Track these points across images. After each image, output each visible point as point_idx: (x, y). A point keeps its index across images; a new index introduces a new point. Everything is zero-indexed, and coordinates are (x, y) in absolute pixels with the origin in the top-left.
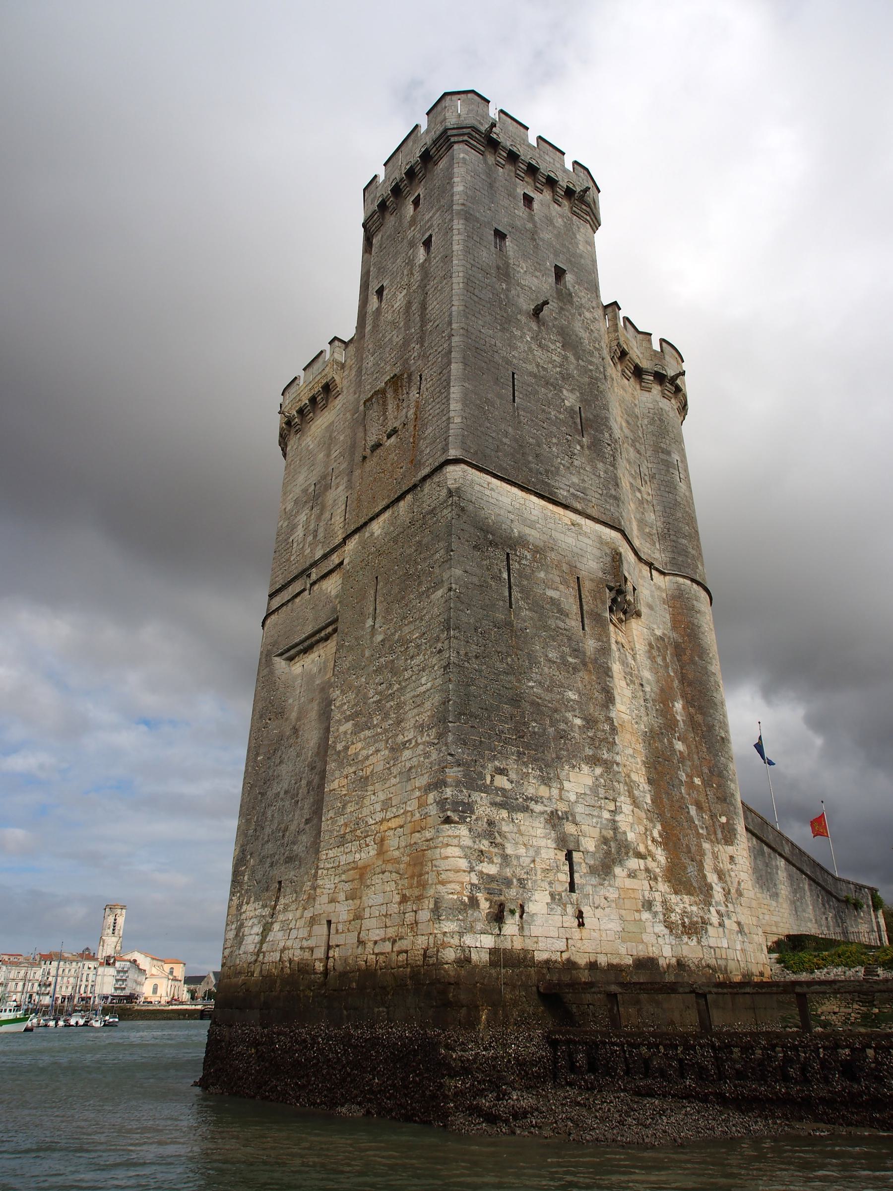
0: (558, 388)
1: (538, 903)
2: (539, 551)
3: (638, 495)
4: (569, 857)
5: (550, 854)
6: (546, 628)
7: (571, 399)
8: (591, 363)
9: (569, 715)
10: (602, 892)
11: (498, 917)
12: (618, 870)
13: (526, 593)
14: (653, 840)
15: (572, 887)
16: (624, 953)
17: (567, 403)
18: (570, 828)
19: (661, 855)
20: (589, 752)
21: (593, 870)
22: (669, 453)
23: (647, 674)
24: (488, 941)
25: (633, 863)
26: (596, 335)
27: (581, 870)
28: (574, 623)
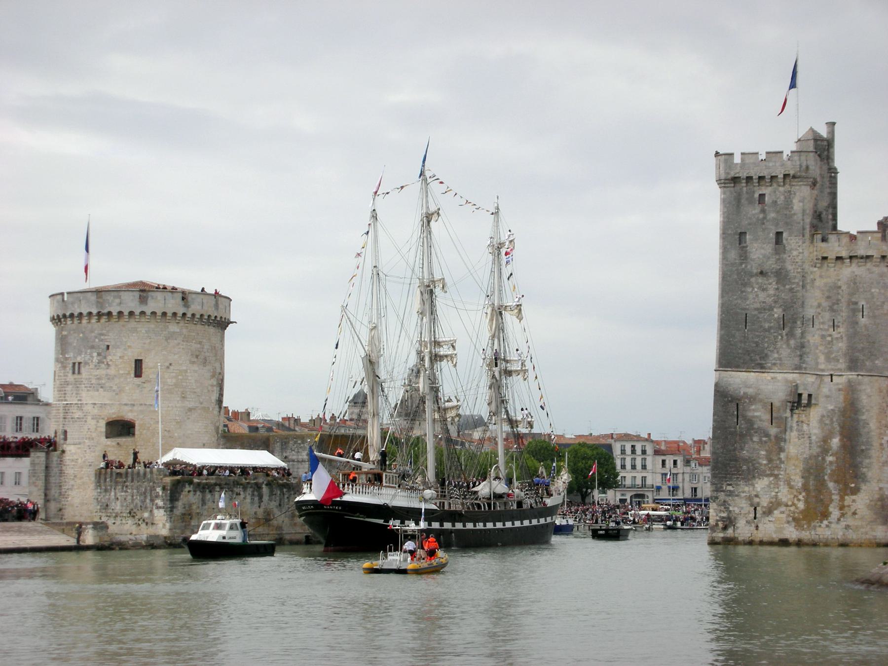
0: (771, 309)
1: (741, 523)
2: (753, 399)
3: (829, 339)
4: (755, 509)
5: (748, 509)
6: (753, 429)
7: (778, 312)
8: (794, 283)
9: (760, 461)
10: (767, 519)
11: (725, 528)
12: (775, 512)
13: (744, 417)
14: (799, 500)
15: (755, 518)
16: (776, 537)
17: (776, 316)
18: (756, 500)
19: (801, 505)
20: (768, 472)
21: (764, 513)
22: (856, 303)
23: (816, 431)
24: (721, 535)
25: (783, 509)
26: (800, 263)
28: (766, 424)
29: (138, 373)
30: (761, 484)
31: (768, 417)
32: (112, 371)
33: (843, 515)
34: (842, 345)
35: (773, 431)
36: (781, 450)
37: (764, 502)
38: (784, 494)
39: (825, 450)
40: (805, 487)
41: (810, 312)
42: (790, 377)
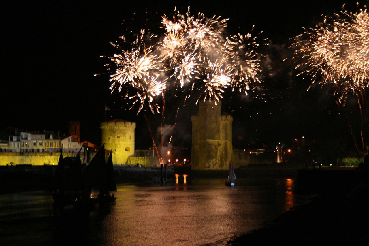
1: (211, 167)
2: (213, 145)
5: (212, 164)
11: (209, 168)
16: (216, 169)
19: (220, 163)
27: (214, 165)
29: (130, 138)
30: (214, 160)
31: (215, 148)
32: (126, 138)
33: (225, 165)
34: (224, 135)
35: (216, 150)
36: (217, 154)
37: (215, 163)
38: (218, 162)
39: (223, 154)
40: (220, 160)
41: (221, 129)
42: (218, 141)
